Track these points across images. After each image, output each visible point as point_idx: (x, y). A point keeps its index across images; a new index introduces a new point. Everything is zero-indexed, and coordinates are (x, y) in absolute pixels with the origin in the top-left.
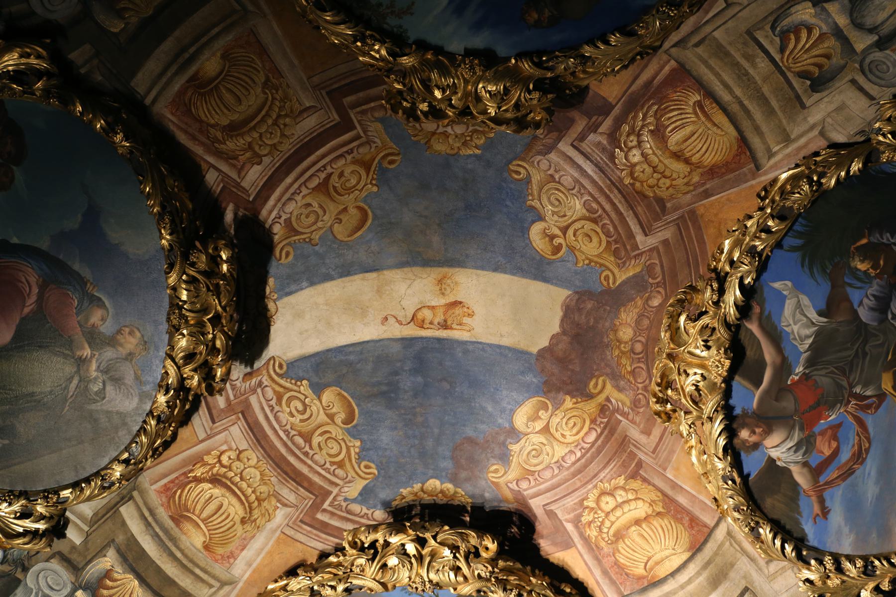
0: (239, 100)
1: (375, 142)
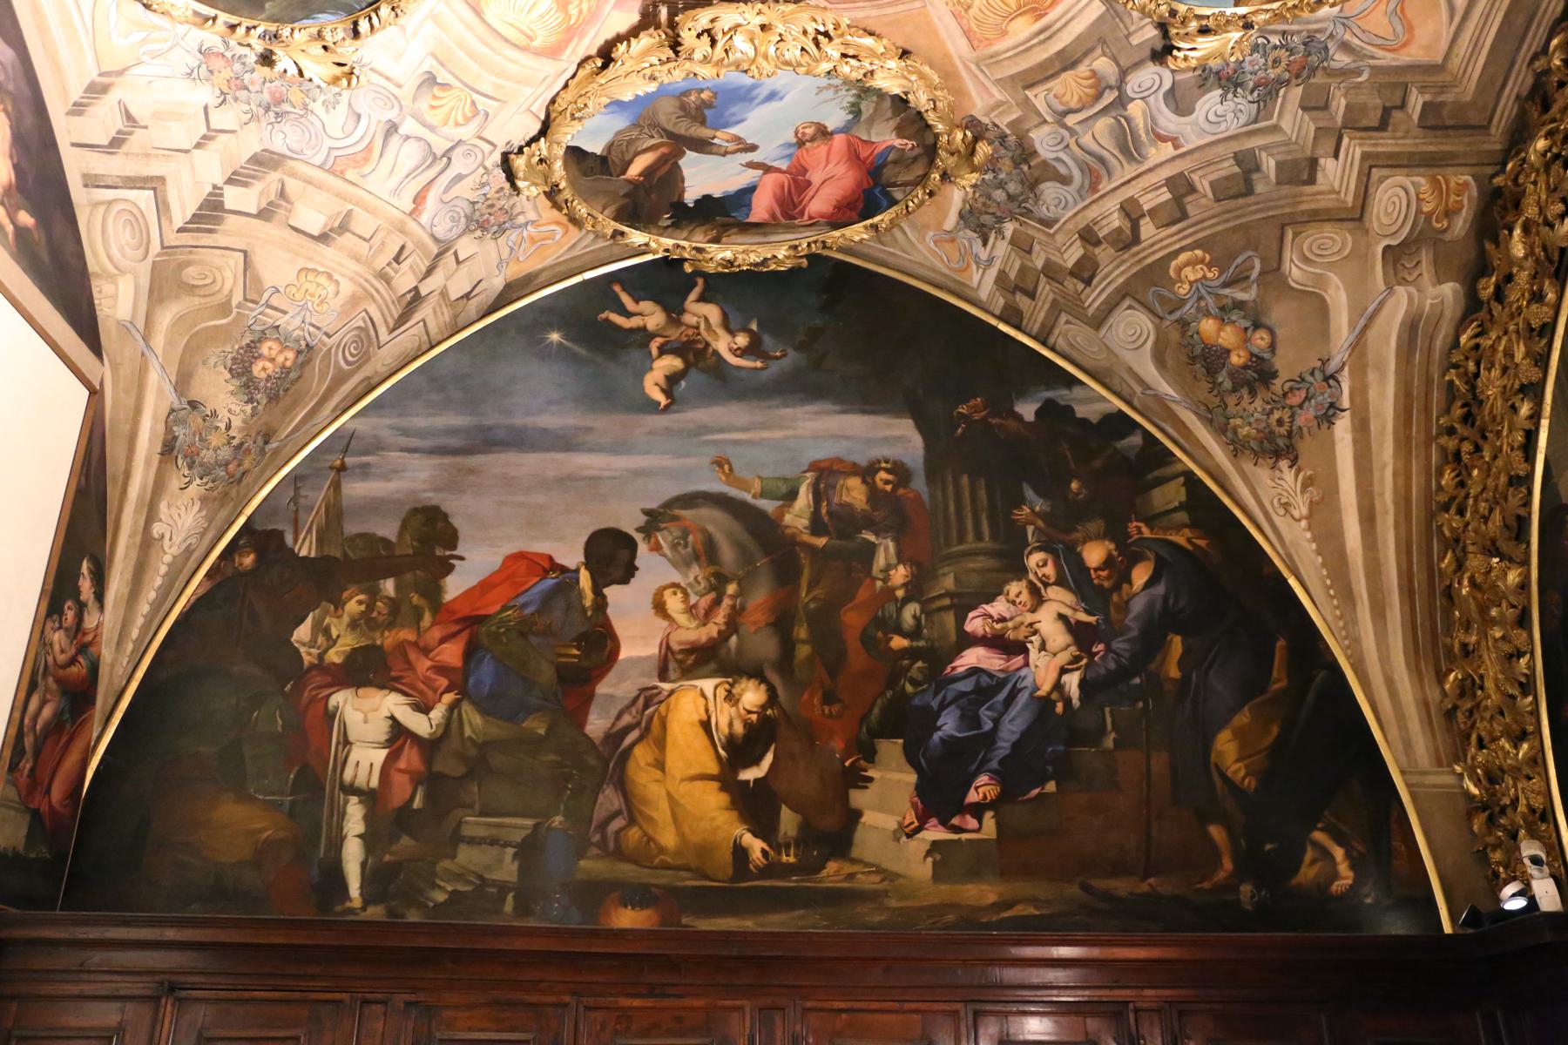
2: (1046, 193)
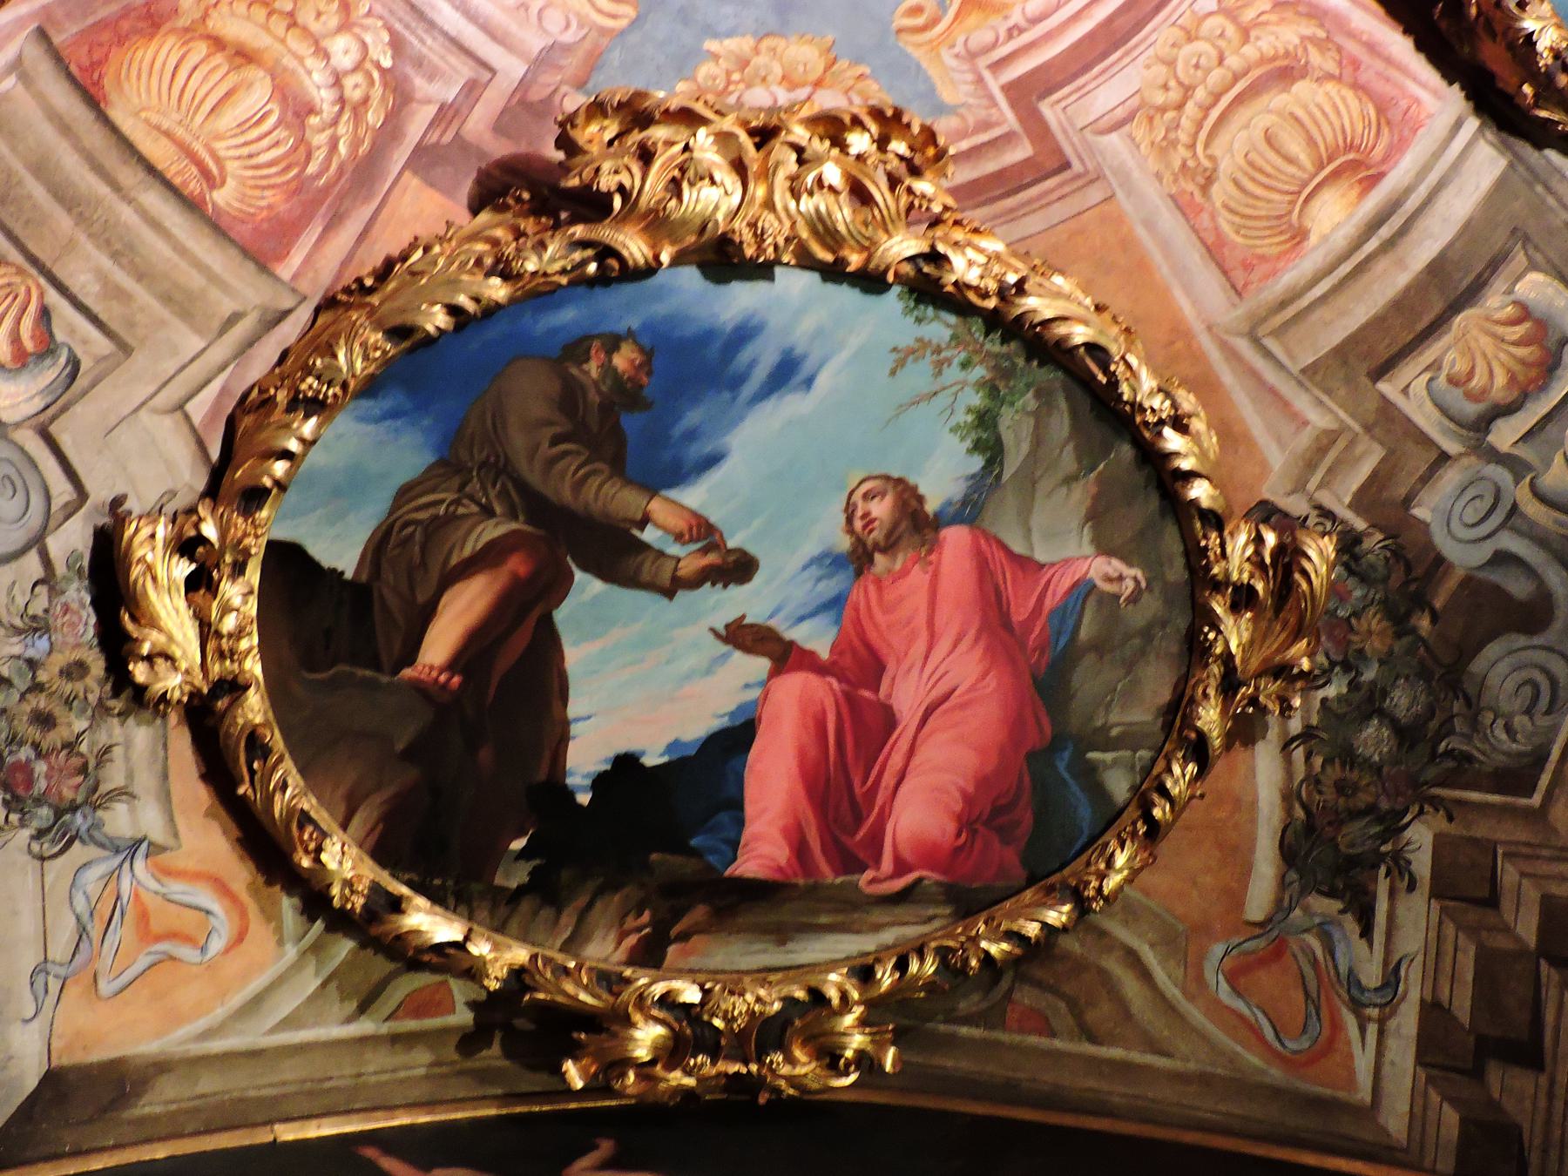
0: (1269, 139)
1: (957, 56)
2: (1493, 679)
